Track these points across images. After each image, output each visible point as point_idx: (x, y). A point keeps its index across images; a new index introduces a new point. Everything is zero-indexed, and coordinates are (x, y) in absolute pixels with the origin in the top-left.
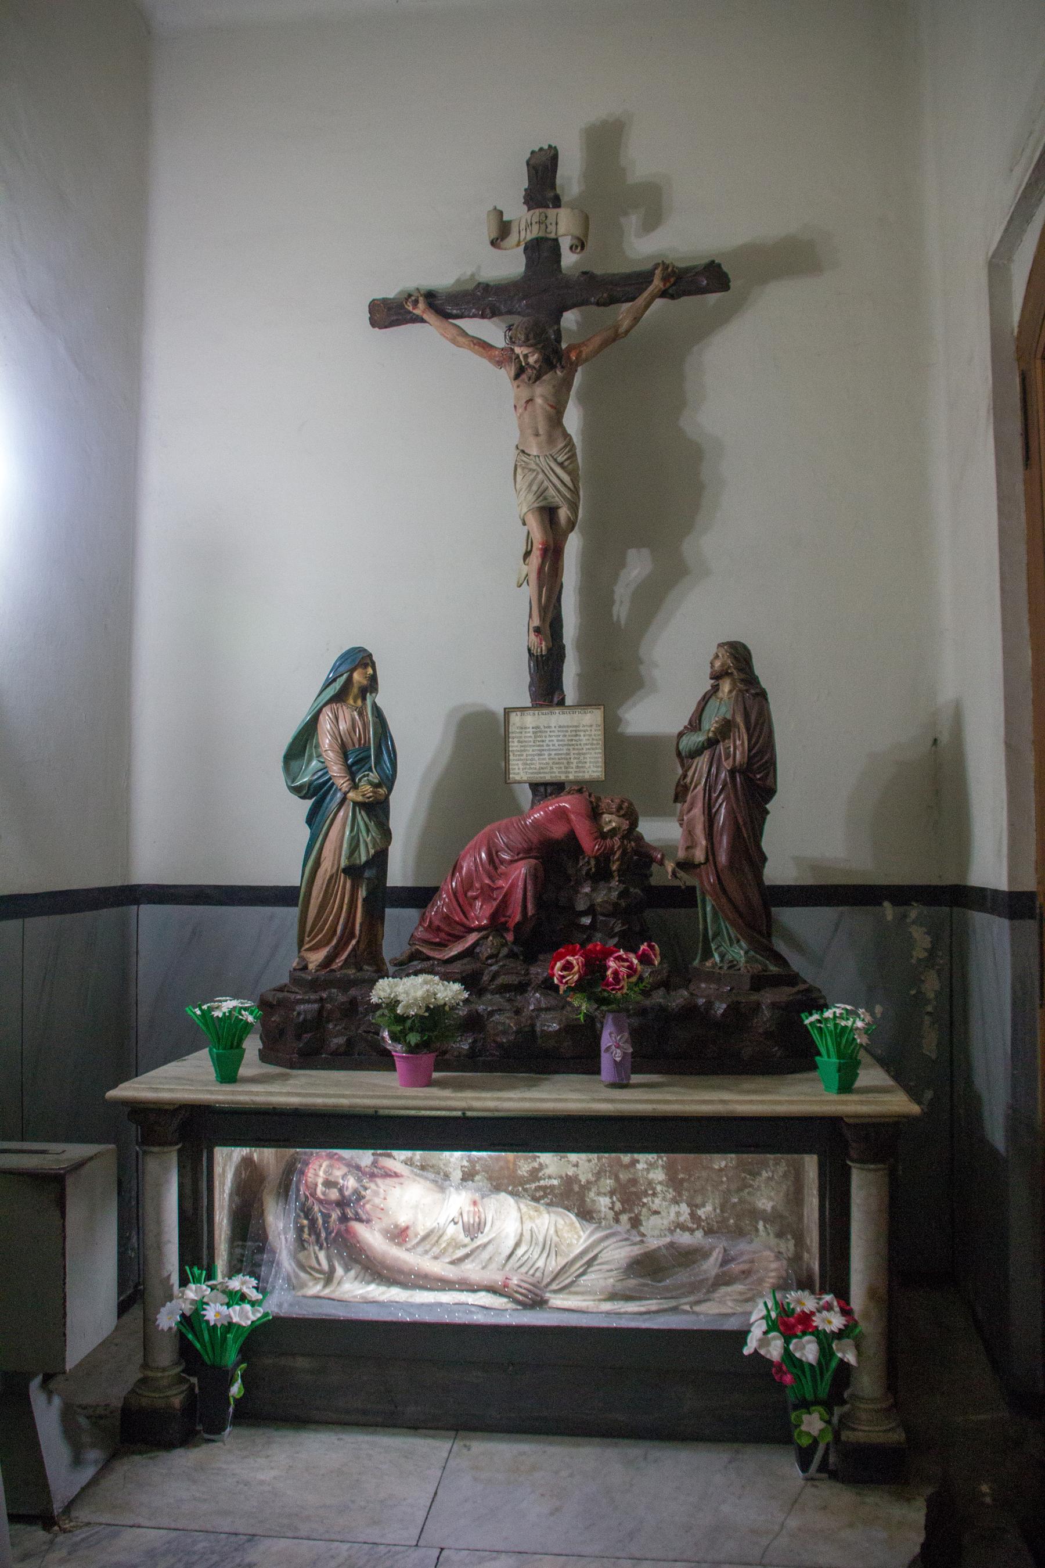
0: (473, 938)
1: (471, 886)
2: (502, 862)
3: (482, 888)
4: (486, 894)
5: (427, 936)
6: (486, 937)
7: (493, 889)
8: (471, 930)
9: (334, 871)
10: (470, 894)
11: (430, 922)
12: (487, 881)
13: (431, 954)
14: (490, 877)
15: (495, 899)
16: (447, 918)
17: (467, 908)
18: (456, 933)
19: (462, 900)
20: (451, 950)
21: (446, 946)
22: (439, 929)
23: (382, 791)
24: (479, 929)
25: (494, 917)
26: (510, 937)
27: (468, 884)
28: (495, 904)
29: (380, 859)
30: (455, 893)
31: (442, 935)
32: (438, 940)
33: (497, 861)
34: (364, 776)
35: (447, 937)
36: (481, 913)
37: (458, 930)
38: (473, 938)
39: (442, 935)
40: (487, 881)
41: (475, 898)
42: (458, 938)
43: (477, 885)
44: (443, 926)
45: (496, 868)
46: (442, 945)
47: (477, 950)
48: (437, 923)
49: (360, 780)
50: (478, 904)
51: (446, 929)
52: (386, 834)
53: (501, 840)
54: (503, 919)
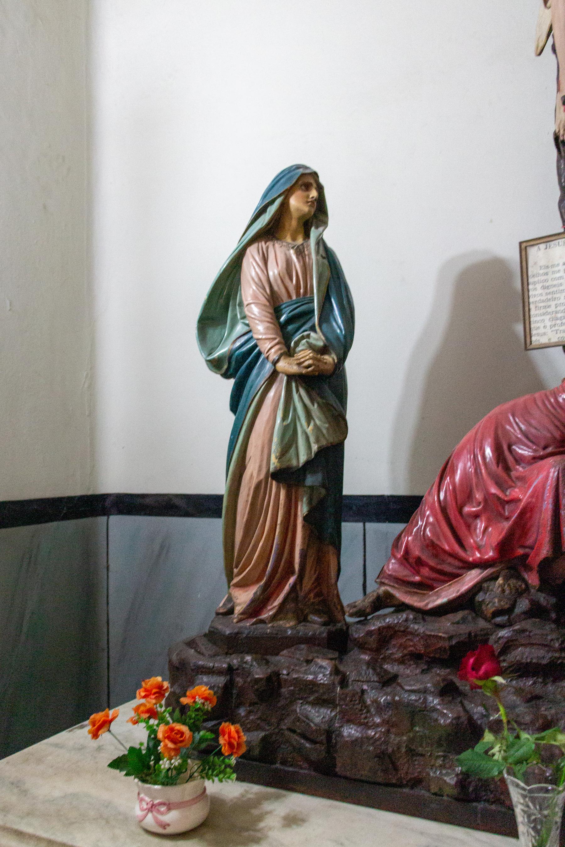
0: (472, 578)
1: (469, 497)
2: (519, 460)
3: (485, 500)
4: (494, 507)
6: (493, 578)
7: (504, 503)
9: (262, 476)
10: (467, 509)
11: (407, 551)
12: (494, 490)
13: (408, 600)
14: (499, 484)
15: (507, 519)
16: (432, 546)
17: (462, 531)
18: (448, 569)
19: (454, 519)
20: (438, 596)
21: (432, 588)
22: (419, 562)
23: (330, 359)
25: (505, 547)
26: (533, 579)
27: (464, 494)
28: (507, 525)
29: (330, 458)
30: (444, 510)
31: (425, 571)
32: (417, 578)
34: (303, 338)
36: (484, 538)
38: (472, 578)
39: (425, 571)
40: (494, 490)
42: (454, 577)
43: (479, 496)
44: (424, 557)
45: (507, 469)
46: (425, 587)
47: (480, 597)
48: (416, 552)
49: (297, 344)
50: (480, 525)
51: (432, 563)
52: (338, 420)
53: (516, 427)
54: (521, 551)
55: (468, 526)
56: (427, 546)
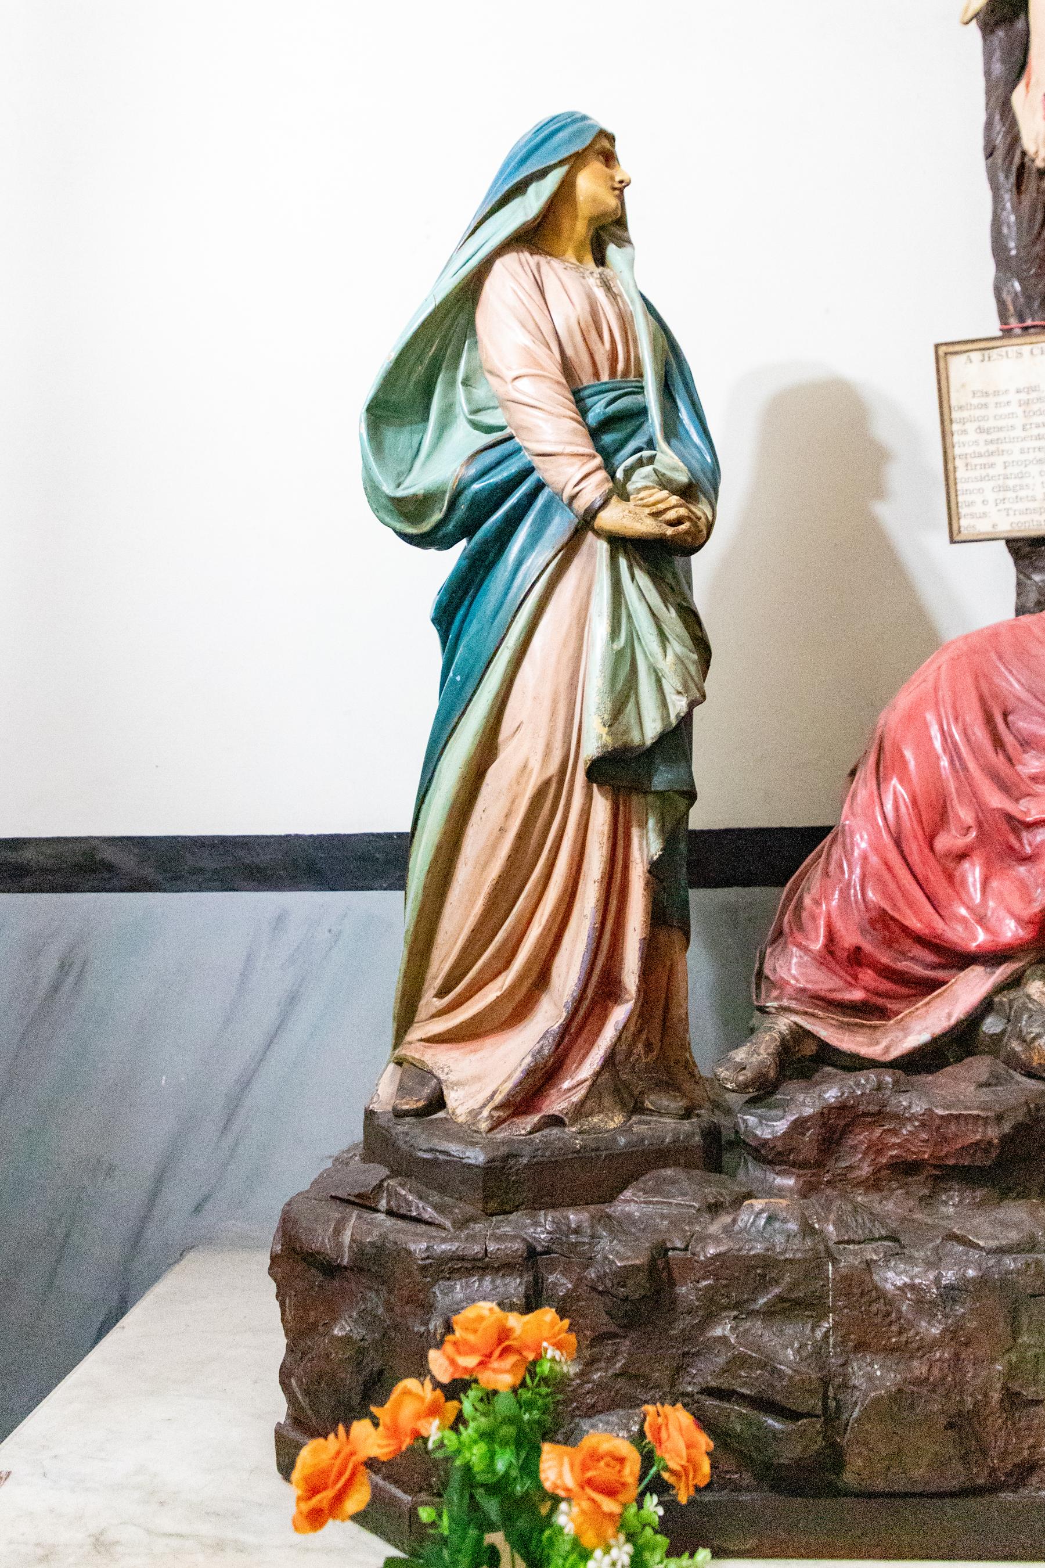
5: (824, 982)
8: (962, 960)
10: (945, 842)
11: (831, 938)
12: (996, 800)
14: (1005, 787)
17: (940, 887)
22: (857, 958)
24: (992, 957)
27: (935, 815)
33: (1009, 739)
35: (886, 985)
37: (917, 963)
40: (996, 800)
41: (963, 856)
43: (965, 814)
44: (868, 947)
48: (850, 938)
51: (885, 958)
55: (950, 877)
56: (872, 922)
